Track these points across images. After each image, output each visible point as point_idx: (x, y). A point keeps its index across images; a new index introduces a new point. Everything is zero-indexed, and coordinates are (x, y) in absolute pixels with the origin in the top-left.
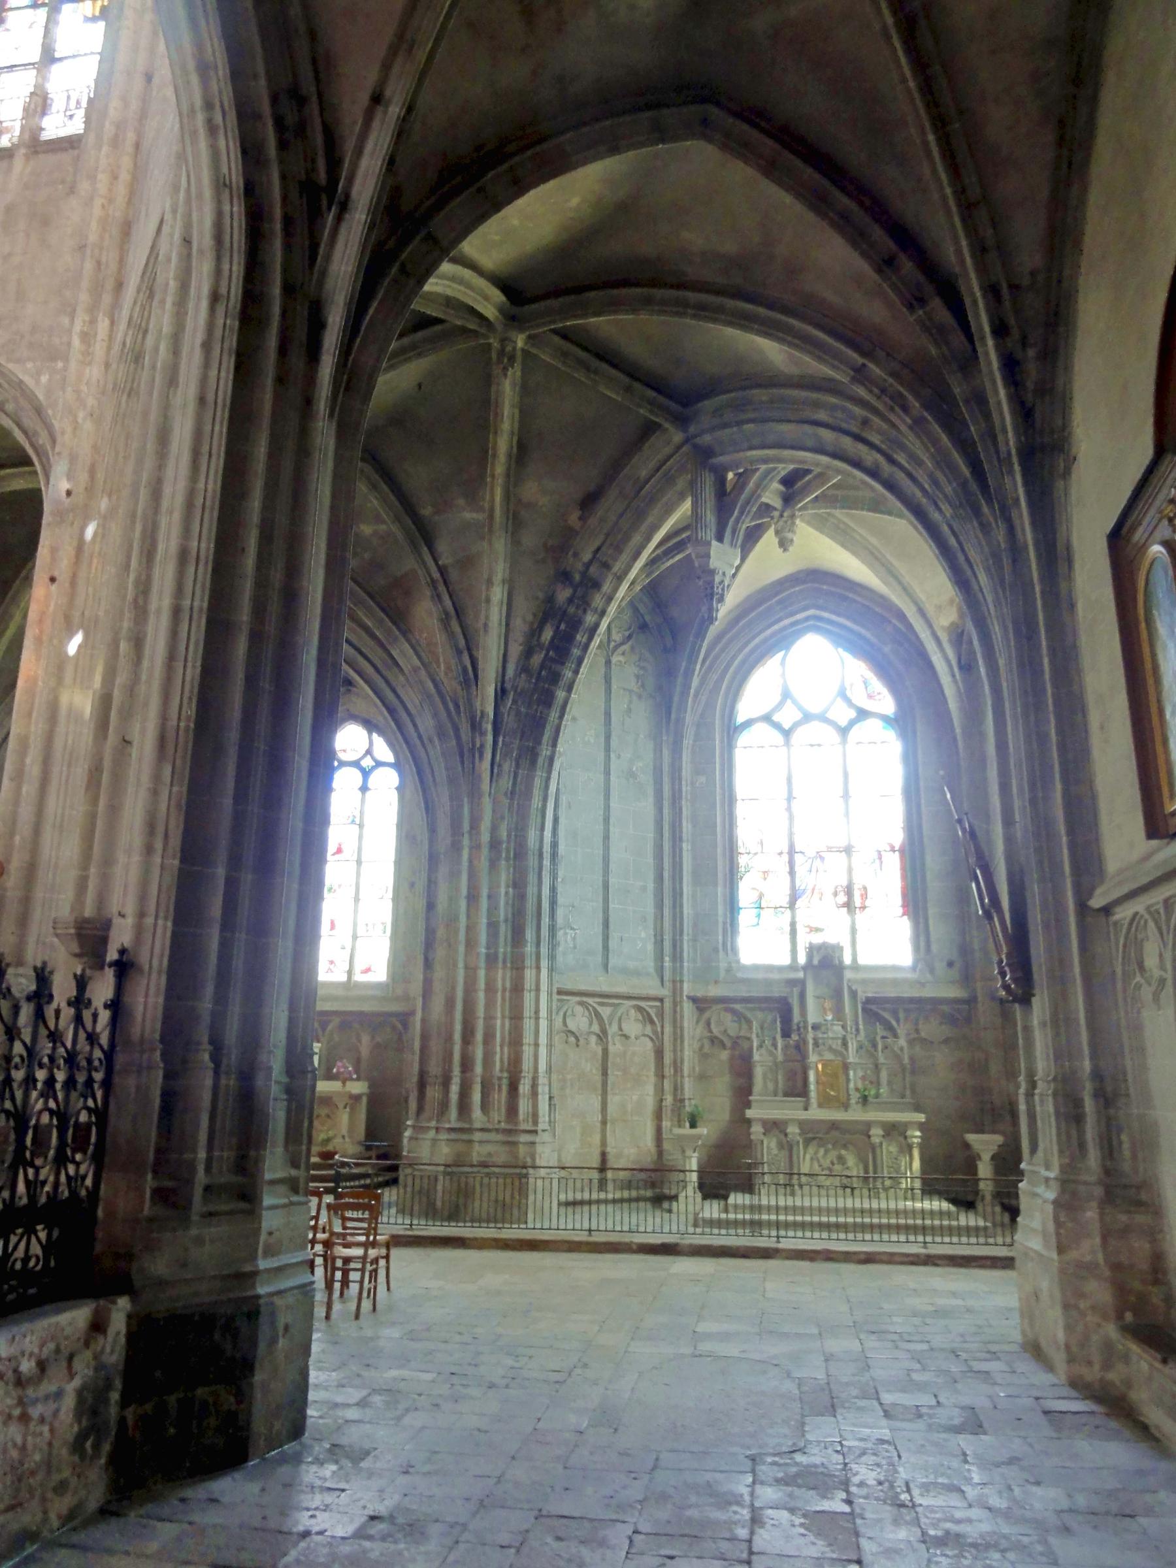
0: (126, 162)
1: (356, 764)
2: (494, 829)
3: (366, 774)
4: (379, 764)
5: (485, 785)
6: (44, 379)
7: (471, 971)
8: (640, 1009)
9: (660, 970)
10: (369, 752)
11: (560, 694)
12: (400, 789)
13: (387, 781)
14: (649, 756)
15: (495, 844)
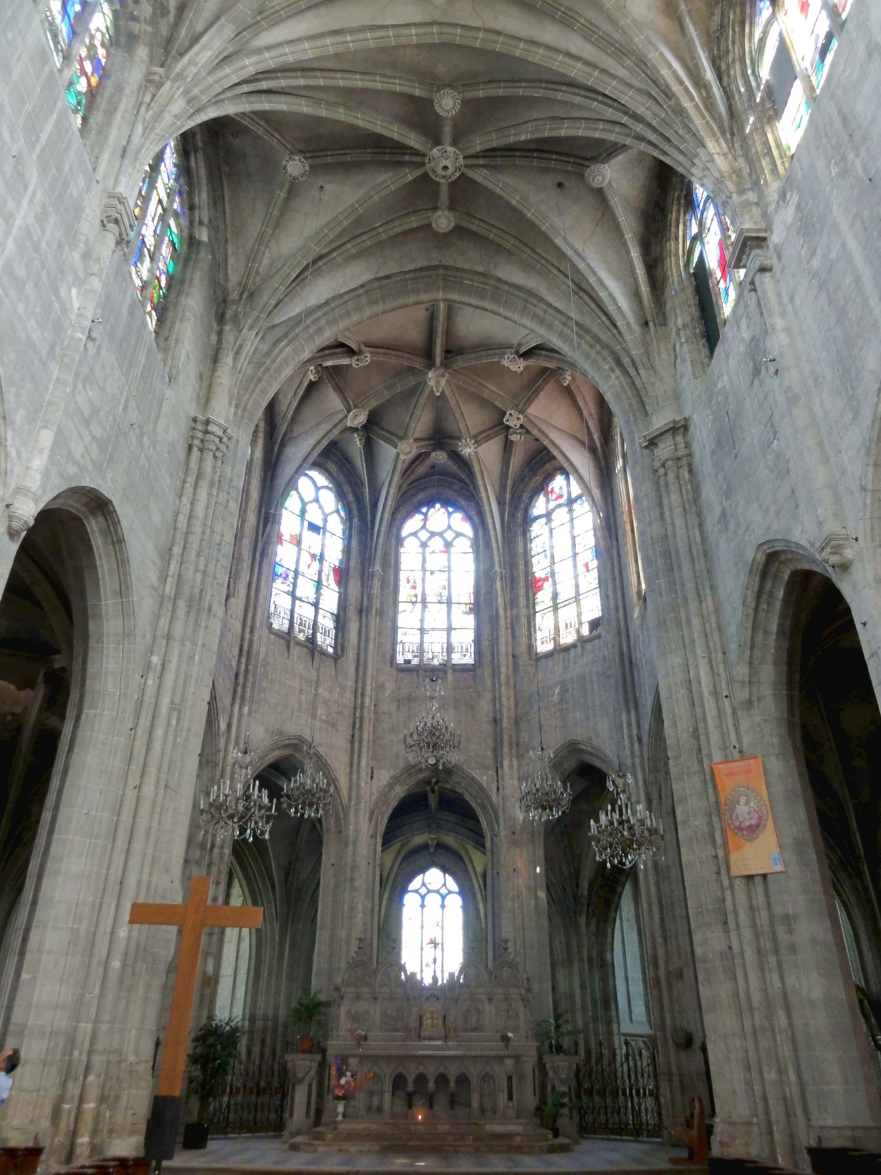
0: (512, 692)
1: (437, 892)
2: (589, 951)
3: (443, 897)
4: (450, 892)
5: (583, 929)
6: (485, 778)
7: (586, 1024)
8: (644, 1042)
9: (649, 1021)
10: (444, 885)
11: (619, 888)
12: (465, 907)
13: (455, 903)
14: (633, 909)
15: (590, 960)
